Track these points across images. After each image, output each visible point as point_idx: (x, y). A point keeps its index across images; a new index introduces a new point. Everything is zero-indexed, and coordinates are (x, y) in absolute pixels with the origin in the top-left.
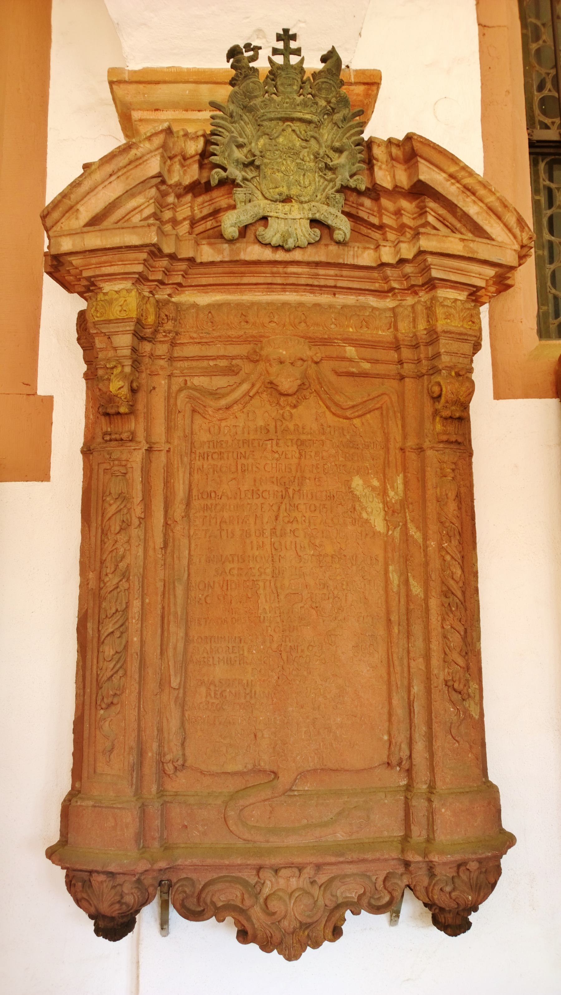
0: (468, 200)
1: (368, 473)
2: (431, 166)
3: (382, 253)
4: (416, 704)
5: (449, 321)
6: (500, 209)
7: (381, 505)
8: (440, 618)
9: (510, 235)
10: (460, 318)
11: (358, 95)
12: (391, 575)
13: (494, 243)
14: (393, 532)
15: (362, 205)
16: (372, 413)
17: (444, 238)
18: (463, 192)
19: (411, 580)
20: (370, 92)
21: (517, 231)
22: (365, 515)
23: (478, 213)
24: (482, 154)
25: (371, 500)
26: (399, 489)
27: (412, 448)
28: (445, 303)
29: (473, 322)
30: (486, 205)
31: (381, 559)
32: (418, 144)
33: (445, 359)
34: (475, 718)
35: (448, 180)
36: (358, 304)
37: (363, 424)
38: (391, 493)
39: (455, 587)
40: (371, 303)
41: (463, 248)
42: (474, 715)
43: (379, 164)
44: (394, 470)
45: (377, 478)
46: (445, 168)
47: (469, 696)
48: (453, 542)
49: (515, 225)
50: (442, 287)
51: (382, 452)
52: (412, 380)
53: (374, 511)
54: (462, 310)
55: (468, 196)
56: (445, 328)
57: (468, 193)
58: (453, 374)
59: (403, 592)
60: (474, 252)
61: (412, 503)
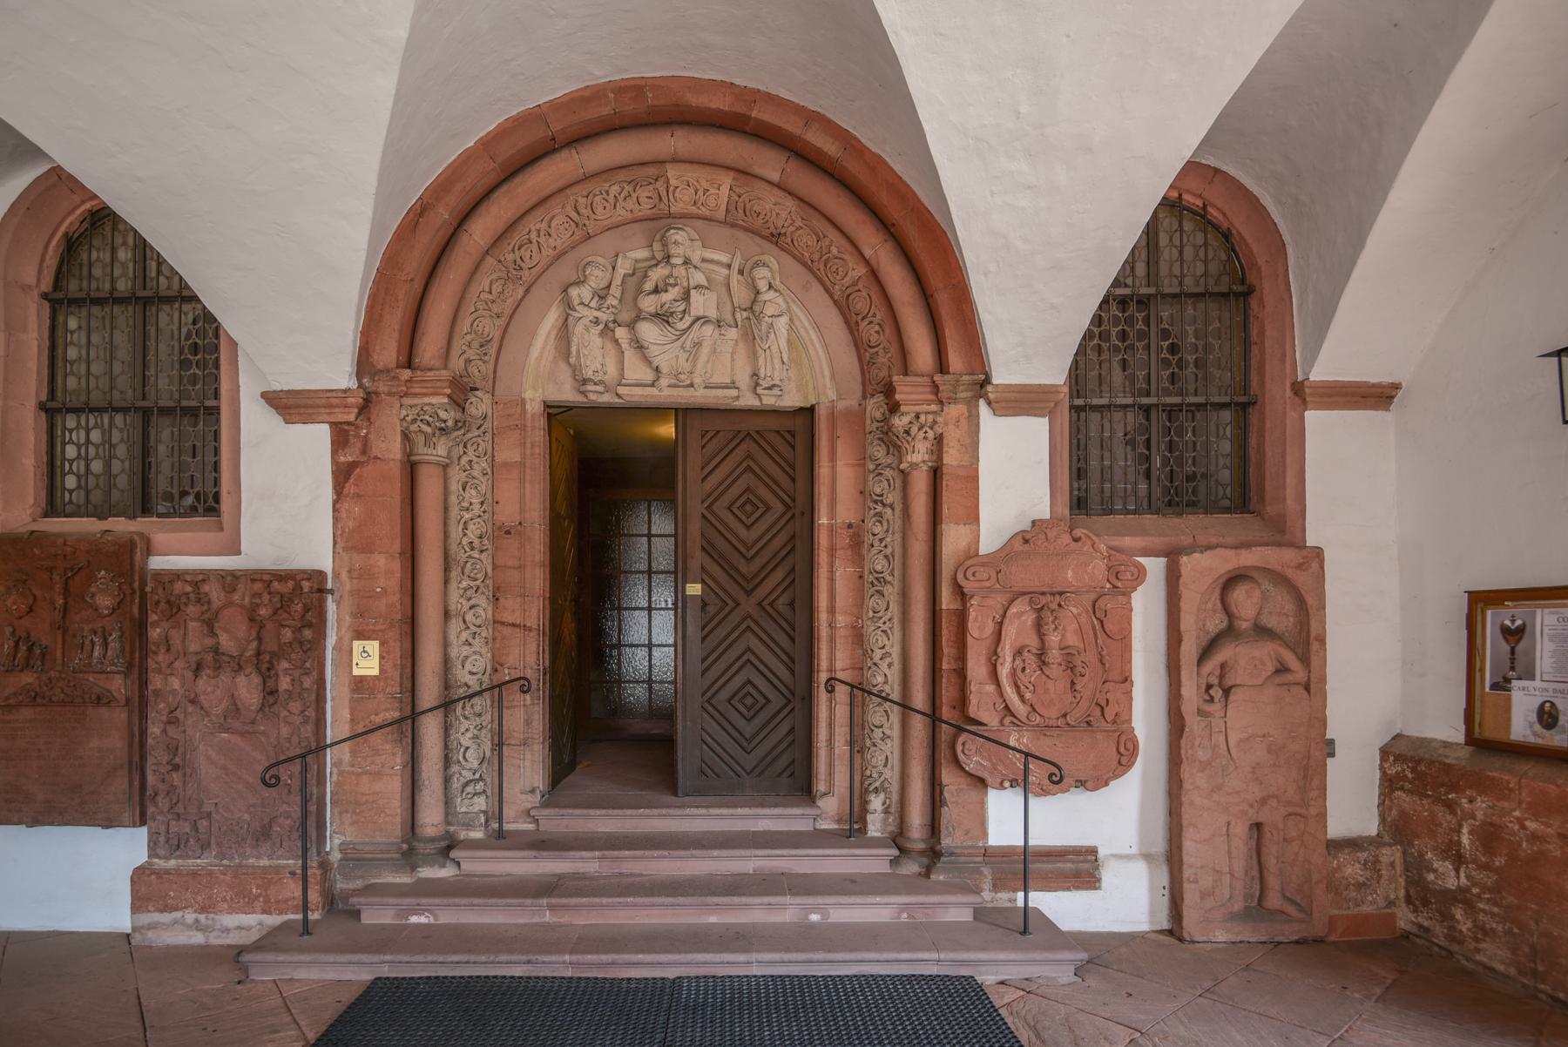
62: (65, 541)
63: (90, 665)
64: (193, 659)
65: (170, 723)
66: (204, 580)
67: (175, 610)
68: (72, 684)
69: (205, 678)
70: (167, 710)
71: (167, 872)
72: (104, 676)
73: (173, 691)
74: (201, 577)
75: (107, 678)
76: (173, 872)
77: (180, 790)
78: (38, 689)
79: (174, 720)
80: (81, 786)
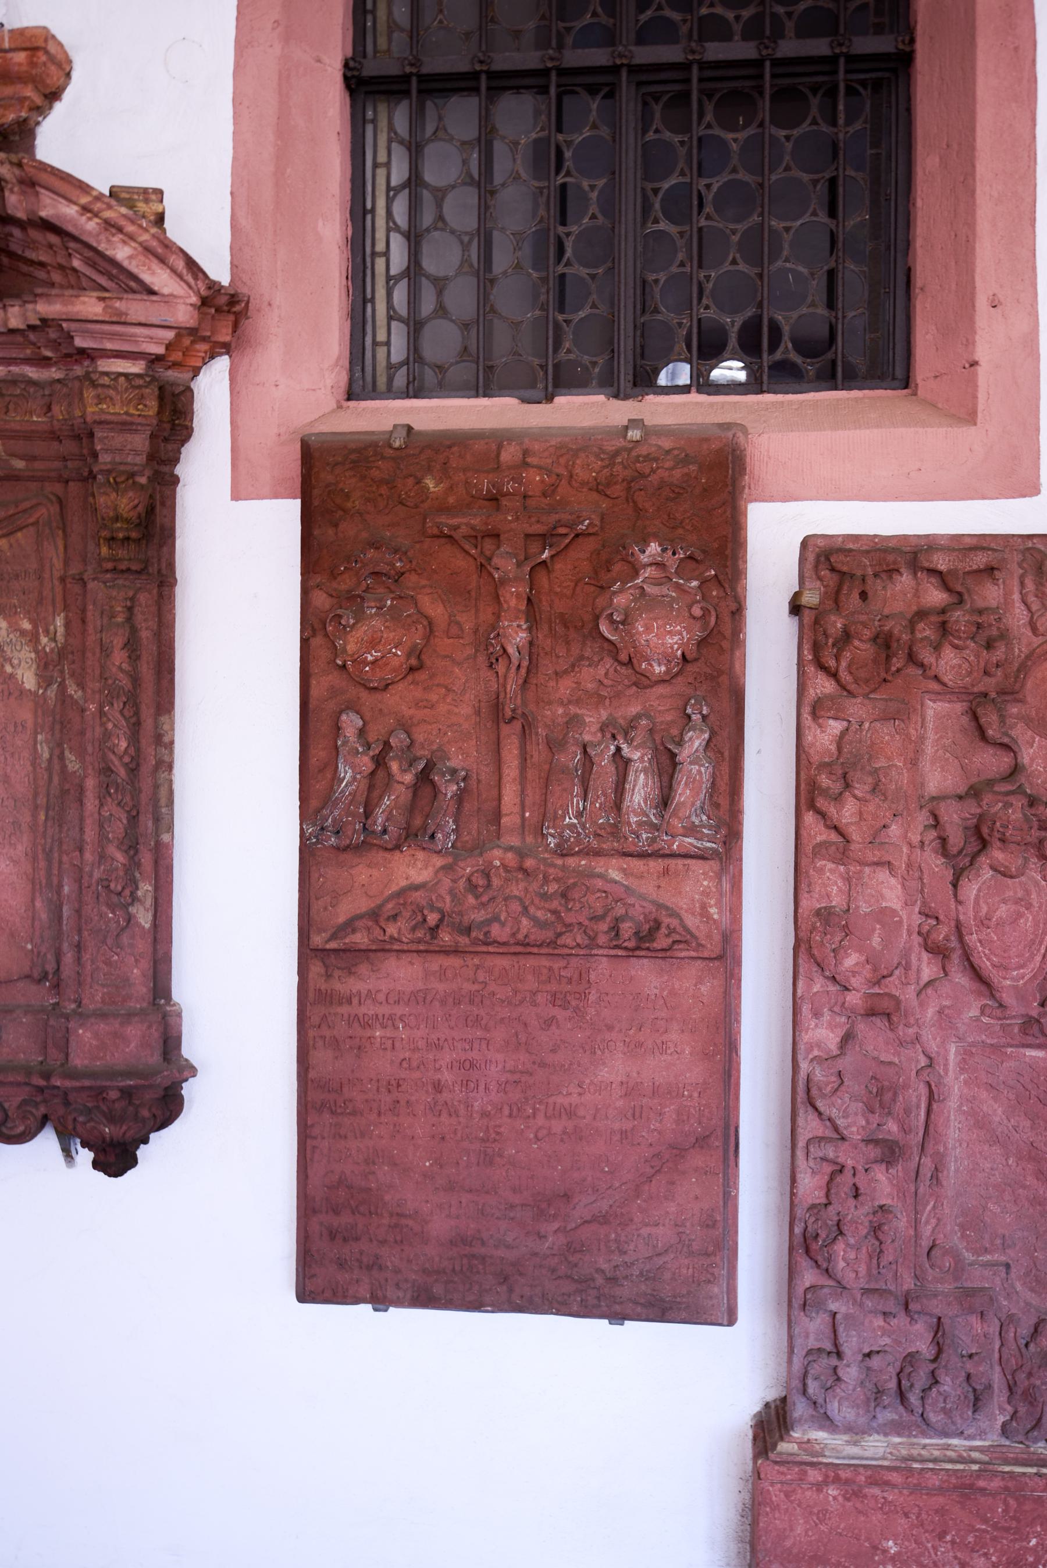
0: (115, 239)
1: (16, 612)
2: (56, 197)
3: (9, 315)
4: (65, 909)
5: (105, 406)
6: (160, 250)
7: (33, 655)
8: (97, 802)
9: (182, 283)
10: (122, 402)
11: (20, 64)
12: (39, 747)
13: (154, 298)
14: (46, 690)
15: (11, 235)
16: (24, 531)
17: (73, 299)
18: (106, 230)
19: (67, 753)
20: (35, 59)
21: (189, 278)
22: (8, 669)
23: (130, 257)
24: (230, 128)
25: (18, 648)
26: (58, 634)
27: (74, 579)
28: (101, 382)
29: (145, 406)
30: (141, 244)
31: (30, 724)
32: (31, 170)
33: (105, 458)
34: (144, 927)
35: (82, 215)
36: (10, 378)
37: (11, 546)
38: (44, 640)
39: (117, 763)
40: (30, 375)
41: (104, 309)
42: (143, 923)
43: (9, 186)
44: (51, 609)
45: (29, 619)
46: (74, 199)
47: (139, 900)
48: (115, 705)
49: (185, 272)
50: (102, 357)
51: (36, 583)
52: (80, 484)
53: (23, 664)
54: (126, 389)
55: (113, 235)
56: (97, 418)
57: (114, 231)
58: (111, 480)
59: (57, 767)
60: (121, 314)
61: (72, 653)
62: (526, 453)
63: (615, 831)
64: (954, 817)
65: (871, 1013)
66: (990, 570)
67: (897, 663)
68: (553, 888)
69: (987, 874)
70: (867, 971)
71: (876, 1475)
72: (656, 865)
73: (883, 915)
74: (980, 560)
75: (666, 872)
76: (895, 1477)
77: (901, 1223)
78: (448, 904)
79: (886, 1004)
80: (567, 1197)
